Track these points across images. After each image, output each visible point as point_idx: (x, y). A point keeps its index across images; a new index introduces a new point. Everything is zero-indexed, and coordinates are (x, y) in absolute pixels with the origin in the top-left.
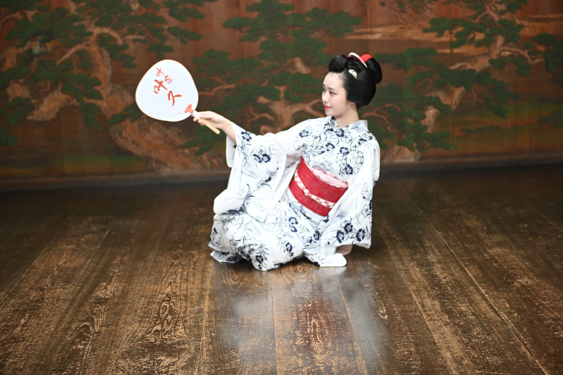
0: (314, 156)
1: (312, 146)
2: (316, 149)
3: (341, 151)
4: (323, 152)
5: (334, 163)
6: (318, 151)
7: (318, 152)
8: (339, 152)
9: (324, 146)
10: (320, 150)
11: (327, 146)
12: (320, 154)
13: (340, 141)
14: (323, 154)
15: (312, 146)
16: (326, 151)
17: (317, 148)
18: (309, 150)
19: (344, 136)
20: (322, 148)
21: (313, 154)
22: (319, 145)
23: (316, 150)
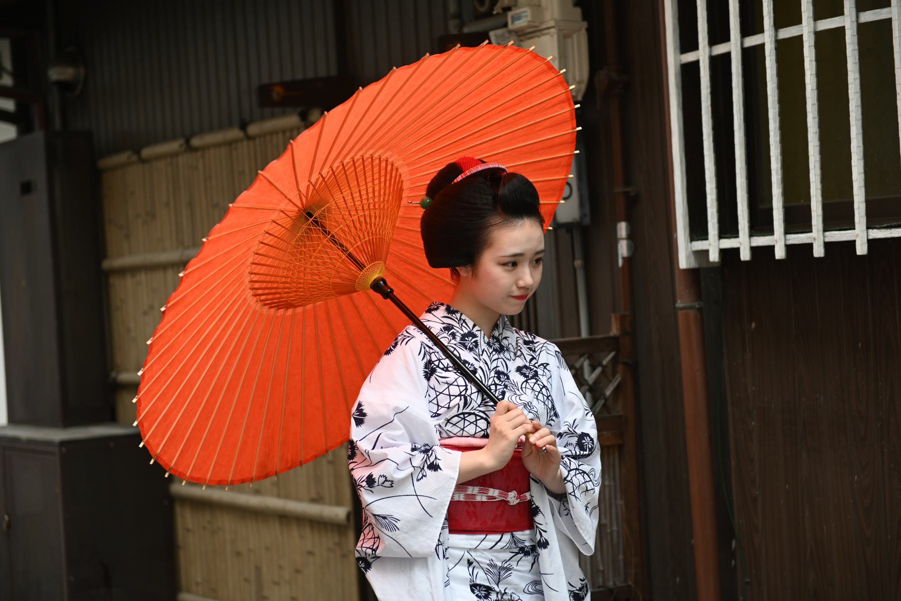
3: (524, 375)
8: (524, 379)
9: (497, 382)
10: (497, 392)
11: (499, 378)
16: (505, 389)
20: (498, 387)
22: (490, 383)
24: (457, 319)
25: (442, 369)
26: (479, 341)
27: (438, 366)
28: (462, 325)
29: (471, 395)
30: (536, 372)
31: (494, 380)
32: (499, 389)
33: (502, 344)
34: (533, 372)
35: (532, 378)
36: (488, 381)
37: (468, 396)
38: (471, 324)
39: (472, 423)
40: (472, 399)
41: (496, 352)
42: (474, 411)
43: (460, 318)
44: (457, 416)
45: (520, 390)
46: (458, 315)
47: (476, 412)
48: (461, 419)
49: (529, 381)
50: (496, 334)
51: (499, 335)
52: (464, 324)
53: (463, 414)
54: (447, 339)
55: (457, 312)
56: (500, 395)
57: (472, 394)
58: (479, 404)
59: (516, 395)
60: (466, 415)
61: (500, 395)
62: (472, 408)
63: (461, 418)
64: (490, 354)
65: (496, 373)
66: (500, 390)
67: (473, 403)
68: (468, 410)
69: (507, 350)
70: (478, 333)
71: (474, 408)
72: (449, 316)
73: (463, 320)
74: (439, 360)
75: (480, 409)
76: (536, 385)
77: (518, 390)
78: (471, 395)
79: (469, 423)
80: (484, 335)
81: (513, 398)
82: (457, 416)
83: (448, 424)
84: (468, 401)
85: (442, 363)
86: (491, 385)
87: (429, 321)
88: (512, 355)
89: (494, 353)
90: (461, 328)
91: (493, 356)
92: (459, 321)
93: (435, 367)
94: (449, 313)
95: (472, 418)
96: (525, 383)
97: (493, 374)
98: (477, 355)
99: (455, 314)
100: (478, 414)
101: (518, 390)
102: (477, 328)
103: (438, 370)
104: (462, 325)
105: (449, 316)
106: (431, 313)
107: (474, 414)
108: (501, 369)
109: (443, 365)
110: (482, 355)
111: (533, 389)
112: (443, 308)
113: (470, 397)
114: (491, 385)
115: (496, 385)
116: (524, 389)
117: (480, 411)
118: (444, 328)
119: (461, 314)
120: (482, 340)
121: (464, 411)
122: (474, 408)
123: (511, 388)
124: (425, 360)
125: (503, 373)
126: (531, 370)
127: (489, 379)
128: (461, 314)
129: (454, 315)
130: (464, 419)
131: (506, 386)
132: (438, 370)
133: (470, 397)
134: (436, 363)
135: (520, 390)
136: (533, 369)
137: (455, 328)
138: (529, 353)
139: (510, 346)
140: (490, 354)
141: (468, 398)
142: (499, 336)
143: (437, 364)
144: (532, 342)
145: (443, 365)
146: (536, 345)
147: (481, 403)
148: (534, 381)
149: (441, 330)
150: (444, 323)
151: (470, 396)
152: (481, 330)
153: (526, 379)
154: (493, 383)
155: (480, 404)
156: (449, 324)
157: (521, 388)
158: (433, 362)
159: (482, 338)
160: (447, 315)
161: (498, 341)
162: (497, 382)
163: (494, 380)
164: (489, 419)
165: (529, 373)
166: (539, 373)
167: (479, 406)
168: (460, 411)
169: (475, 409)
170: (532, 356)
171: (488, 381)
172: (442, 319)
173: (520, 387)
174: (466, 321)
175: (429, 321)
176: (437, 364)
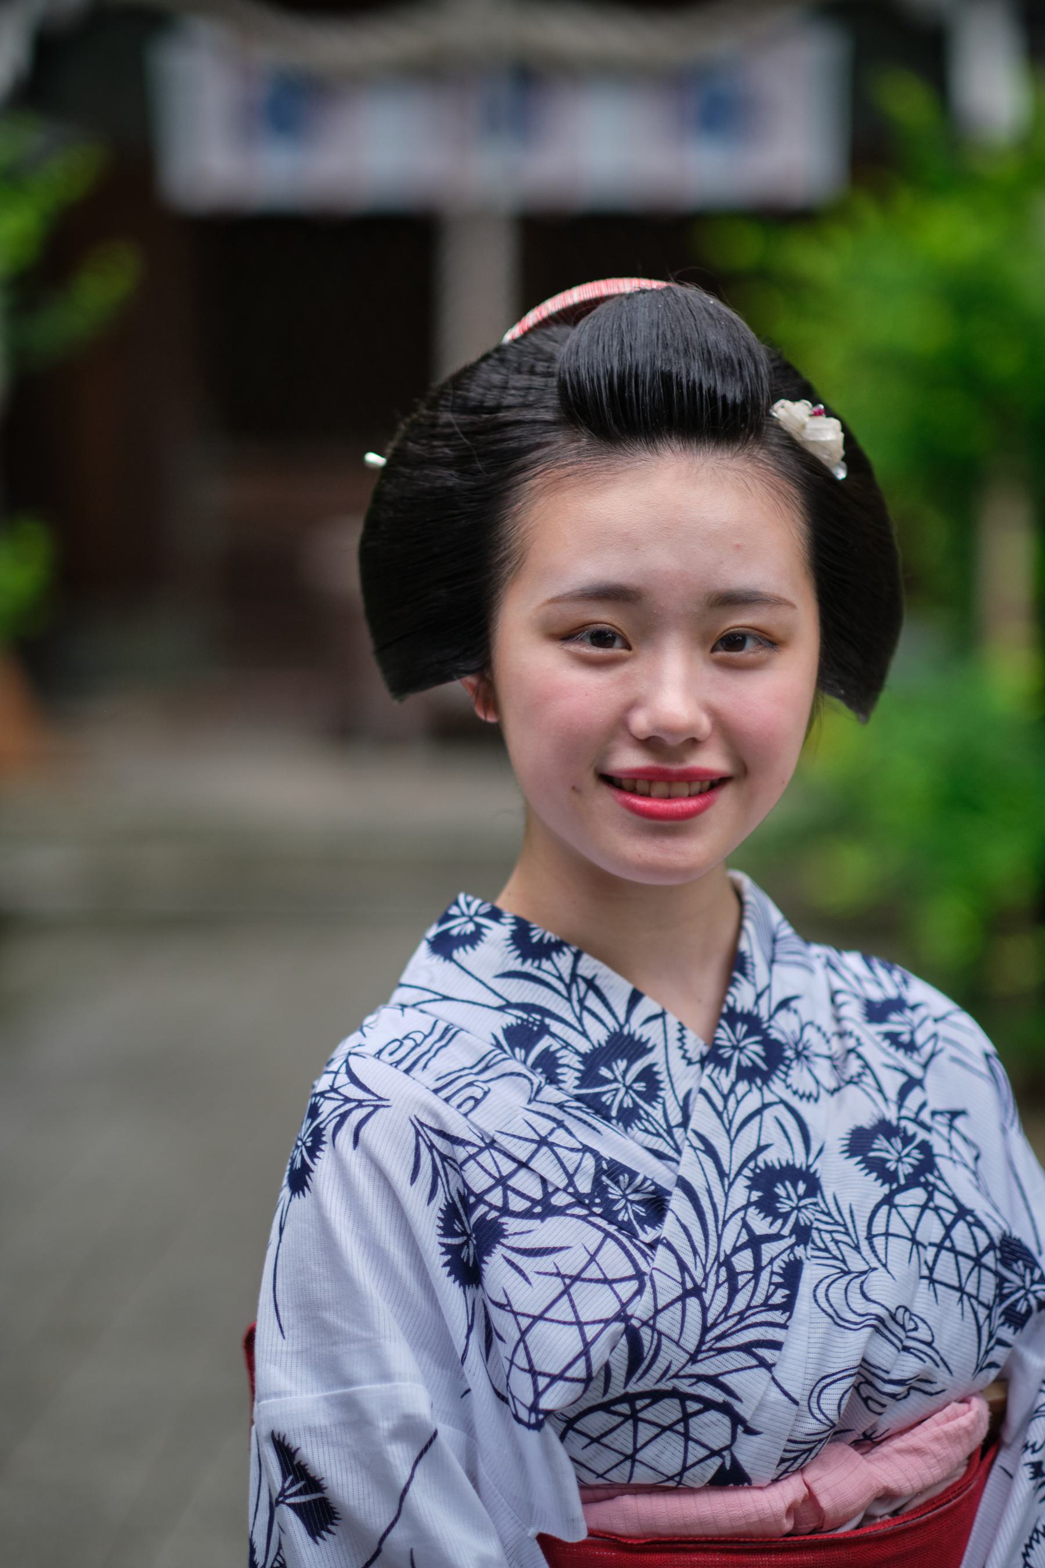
0: (763, 1352)
1: (697, 1291)
2: (733, 1291)
4: (792, 1274)
5: (922, 1301)
6: (758, 1299)
7: (767, 1306)
8: (877, 1190)
9: (761, 1225)
10: (765, 1275)
12: (788, 1306)
13: (804, 1108)
14: (805, 1289)
15: (697, 1291)
17: (733, 1276)
18: (691, 1342)
19: (789, 1053)
20: (768, 1250)
21: (747, 1348)
22: (727, 1246)
23: (740, 1302)
24: (560, 978)
25: (527, 1214)
26: (660, 1068)
27: (505, 1210)
28: (581, 1001)
29: (654, 1317)
30: (925, 1147)
31: (745, 1225)
32: (771, 1261)
33: (775, 1034)
34: (916, 1153)
35: (912, 1181)
36: (719, 1237)
37: (645, 1323)
38: (618, 988)
39: (670, 1428)
40: (660, 1334)
41: (751, 1081)
42: (675, 1381)
43: (574, 976)
44: (605, 1407)
45: (864, 1245)
46: (564, 962)
47: (684, 1386)
48: (619, 1419)
49: (898, 1199)
50: (743, 997)
51: (759, 996)
52: (592, 1001)
54: (526, 1081)
55: (558, 946)
56: (778, 1286)
57: (657, 1312)
58: (691, 1347)
59: (848, 1278)
61: (778, 1286)
62: (668, 1368)
63: (620, 1414)
64: (725, 1098)
65: (755, 1183)
66: (776, 1267)
69: (798, 1055)
70: (652, 1033)
71: (671, 1373)
72: (528, 967)
73: (585, 979)
74: (502, 1181)
75: (699, 1369)
76: (929, 1214)
77: (857, 1248)
78: (654, 1317)
79: (656, 1430)
80: (682, 1029)
81: (836, 1293)
82: (605, 1407)
84: (646, 1349)
85: (514, 1190)
86: (736, 1250)
87: (445, 998)
88: (823, 1069)
89: (742, 1087)
90: (580, 1020)
91: (738, 1102)
92: (568, 987)
93: (494, 1214)
94: (524, 957)
95: (668, 1411)
96: (885, 1209)
97: (740, 1194)
98: (658, 1135)
99: (549, 958)
100: (690, 1390)
101: (857, 1248)
102: (648, 1006)
103: (511, 1225)
104: (581, 1001)
105: (528, 967)
106: (448, 957)
107: (674, 1393)
108: (772, 1157)
109: (523, 1196)
110: (684, 1124)
111: (914, 1242)
112: (499, 933)
113: (653, 1328)
114: (736, 1250)
115: (755, 1242)
116: (879, 1242)
117: (701, 1378)
118: (509, 1032)
119: (577, 956)
120: (675, 1054)
121: (633, 1388)
122: (671, 1373)
123: (827, 1237)
124: (440, 1201)
125: (791, 1173)
126: (907, 1140)
127: (725, 1223)
128: (577, 956)
129: (546, 965)
130: (634, 1417)
131: (803, 1234)
132: (511, 1225)
133: (653, 1328)
134: (495, 1197)
135: (864, 1245)
136: (914, 1136)
137: (555, 1027)
138: (891, 1062)
139: (810, 1033)
140: (725, 1098)
141: (646, 1334)
142: (756, 1003)
143: (499, 1203)
144: (898, 1005)
145: (523, 1196)
146: (915, 1017)
147: (702, 1342)
148: (918, 1195)
149: (499, 1045)
150: (507, 1006)
151: (649, 1323)
152: (662, 1015)
153: (886, 1189)
154: (744, 1237)
155: (698, 1350)
156: (528, 1008)
157: (870, 1237)
158: (480, 1198)
159: (673, 1044)
160: (516, 965)
161: (753, 1024)
162: (761, 1225)
163: (745, 1225)
164: (738, 1407)
165: (899, 1160)
166: (936, 1150)
167: (693, 1359)
169: (676, 1376)
170: (904, 1071)
171: (719, 1237)
172: (500, 985)
173: (862, 1233)
174: (598, 982)
175: (445, 998)
176: (499, 1203)
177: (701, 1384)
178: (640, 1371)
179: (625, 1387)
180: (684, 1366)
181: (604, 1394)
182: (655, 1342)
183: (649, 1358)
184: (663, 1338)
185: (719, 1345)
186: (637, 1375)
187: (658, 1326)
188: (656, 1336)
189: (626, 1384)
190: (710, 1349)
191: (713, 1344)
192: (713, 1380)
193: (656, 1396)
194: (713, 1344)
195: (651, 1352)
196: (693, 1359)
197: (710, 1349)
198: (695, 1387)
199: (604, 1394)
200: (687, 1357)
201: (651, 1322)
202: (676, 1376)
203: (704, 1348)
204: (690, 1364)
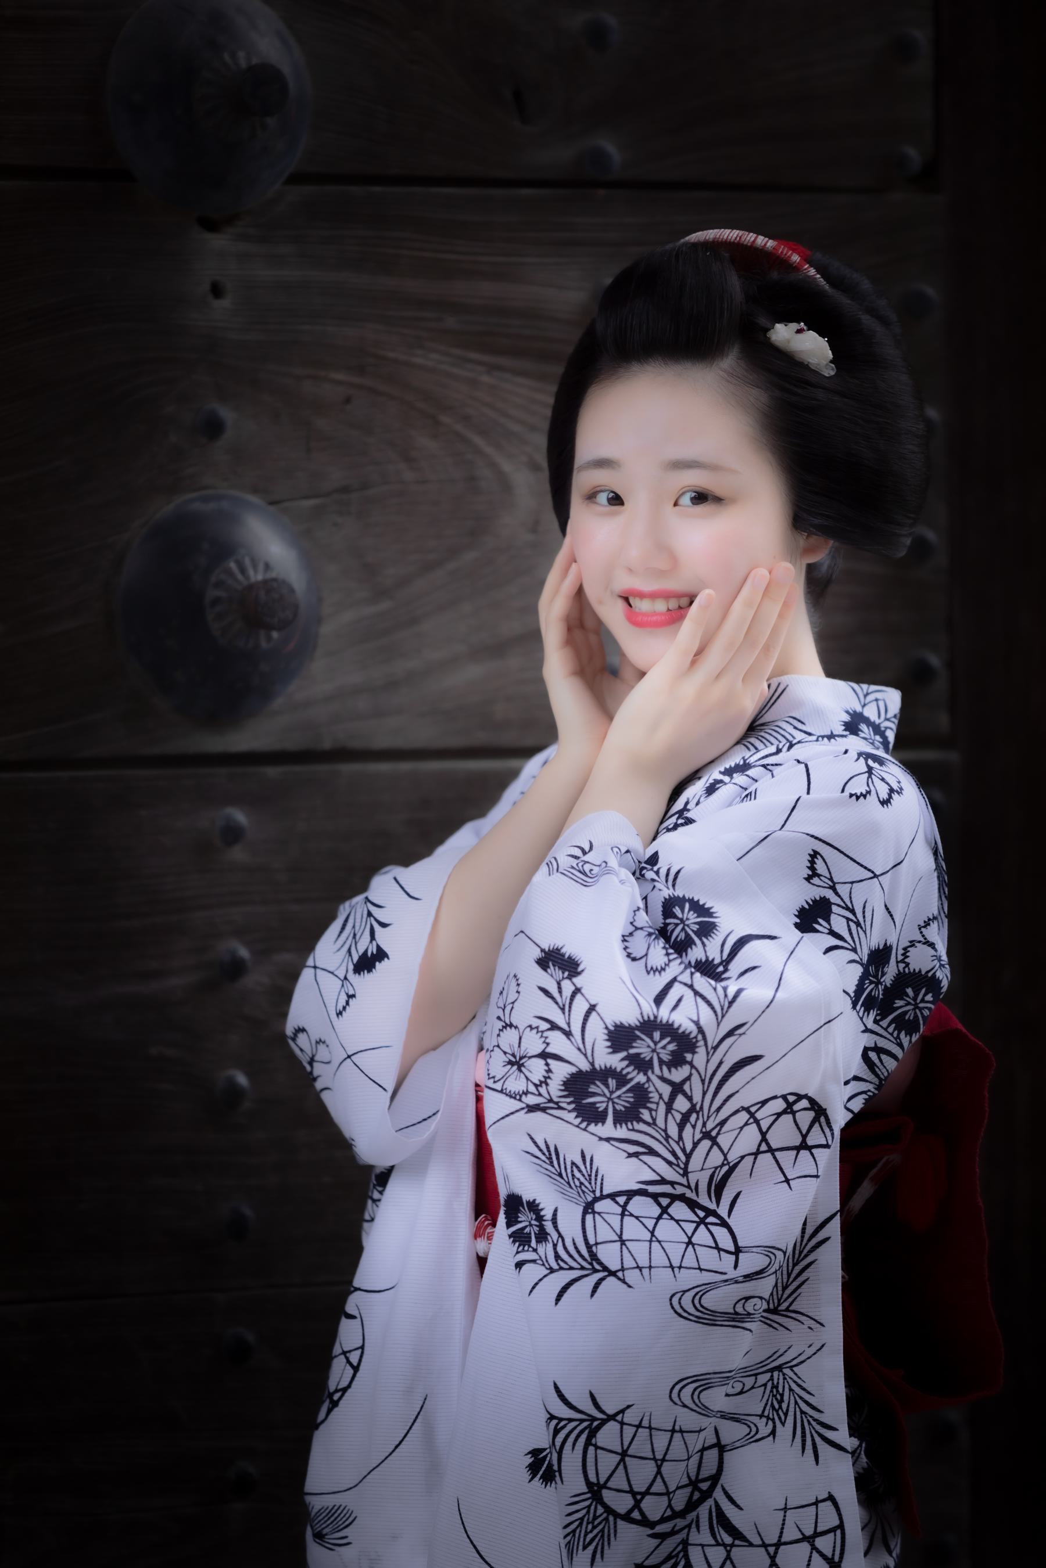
29: (729, 1552)
37: (732, 1545)
40: (718, 1544)
47: (680, 1523)
53: (707, 1494)
60: (697, 1495)
67: (705, 1537)
68: (703, 1511)
71: (694, 1526)
78: (729, 1552)
83: (715, 1441)
84: (722, 1532)
107: (682, 1514)
113: (725, 1545)
117: (673, 1533)
121: (710, 1502)
122: (694, 1526)
133: (725, 1545)
141: (728, 1540)
147: (686, 1557)
155: (685, 1550)
168: (718, 1493)
169: (689, 1526)
177: (669, 1530)
178: (714, 1514)
179: (715, 1499)
180: (688, 1535)
181: (722, 1486)
182: (718, 1537)
183: (715, 1526)
184: (713, 1542)
185: (673, 1561)
186: (714, 1510)
187: (722, 1548)
188: (720, 1541)
189: (716, 1502)
190: (677, 1555)
191: (677, 1560)
192: (663, 1537)
193: (692, 1505)
194: (677, 1560)
195: (716, 1529)
196: (685, 1543)
197: (677, 1555)
198: (672, 1525)
199: (722, 1486)
200: (690, 1542)
201: (728, 1548)
202: (689, 1526)
203: (681, 1554)
204: (685, 1539)
